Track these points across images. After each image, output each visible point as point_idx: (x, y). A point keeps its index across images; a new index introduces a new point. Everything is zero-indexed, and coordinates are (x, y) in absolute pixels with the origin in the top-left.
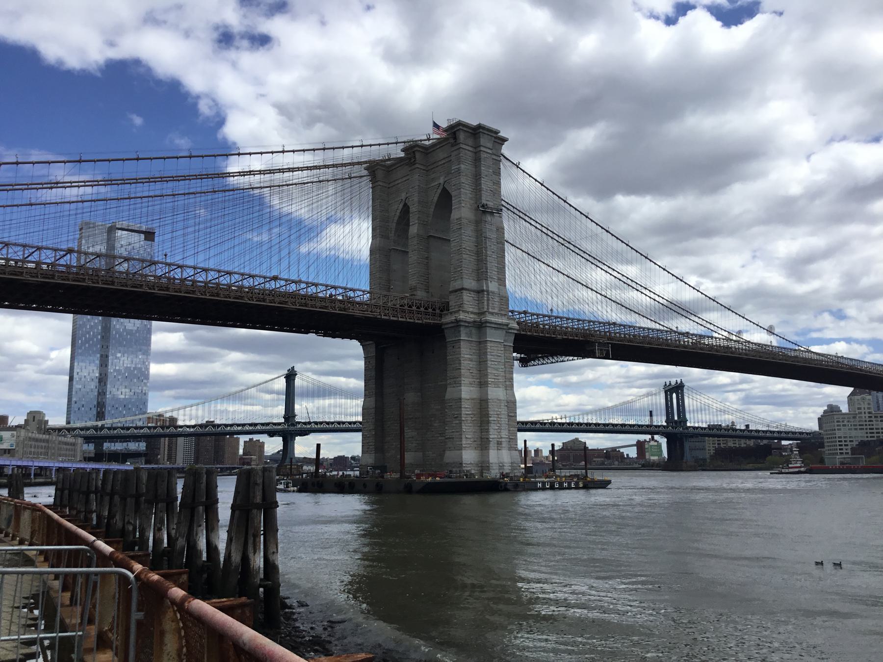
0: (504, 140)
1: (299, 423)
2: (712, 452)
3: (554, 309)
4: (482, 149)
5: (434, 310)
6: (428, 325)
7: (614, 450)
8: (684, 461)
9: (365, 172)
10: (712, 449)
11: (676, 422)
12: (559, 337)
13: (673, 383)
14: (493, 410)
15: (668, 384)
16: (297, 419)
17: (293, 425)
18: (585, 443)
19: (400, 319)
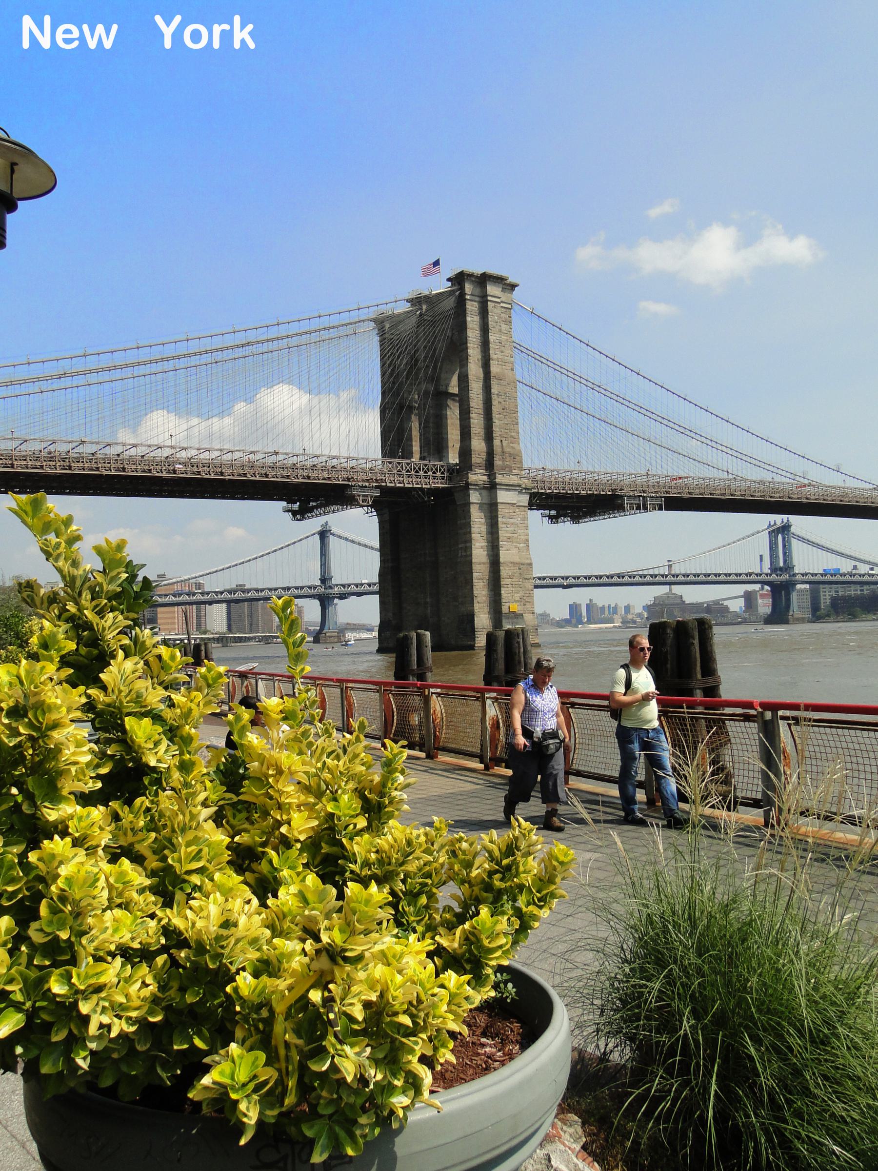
0: (513, 287)
1: (337, 585)
2: (828, 601)
3: (584, 462)
4: (489, 298)
5: (442, 473)
6: (437, 489)
7: (717, 602)
8: (791, 613)
9: (373, 324)
10: (828, 597)
11: (781, 569)
12: (583, 493)
13: (779, 524)
14: (504, 571)
15: (772, 523)
16: (334, 582)
17: (331, 588)
18: (681, 597)
19: (407, 486)
